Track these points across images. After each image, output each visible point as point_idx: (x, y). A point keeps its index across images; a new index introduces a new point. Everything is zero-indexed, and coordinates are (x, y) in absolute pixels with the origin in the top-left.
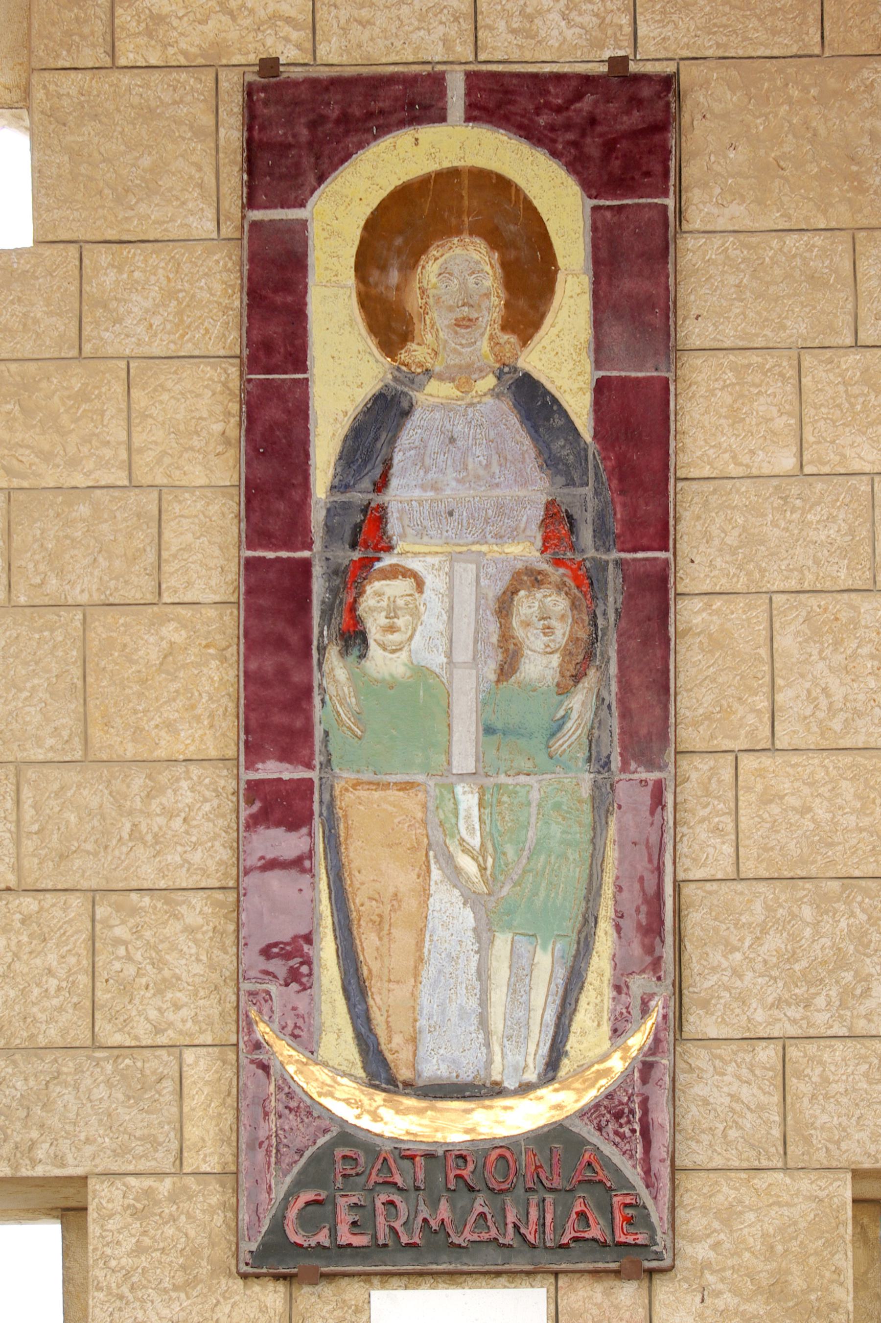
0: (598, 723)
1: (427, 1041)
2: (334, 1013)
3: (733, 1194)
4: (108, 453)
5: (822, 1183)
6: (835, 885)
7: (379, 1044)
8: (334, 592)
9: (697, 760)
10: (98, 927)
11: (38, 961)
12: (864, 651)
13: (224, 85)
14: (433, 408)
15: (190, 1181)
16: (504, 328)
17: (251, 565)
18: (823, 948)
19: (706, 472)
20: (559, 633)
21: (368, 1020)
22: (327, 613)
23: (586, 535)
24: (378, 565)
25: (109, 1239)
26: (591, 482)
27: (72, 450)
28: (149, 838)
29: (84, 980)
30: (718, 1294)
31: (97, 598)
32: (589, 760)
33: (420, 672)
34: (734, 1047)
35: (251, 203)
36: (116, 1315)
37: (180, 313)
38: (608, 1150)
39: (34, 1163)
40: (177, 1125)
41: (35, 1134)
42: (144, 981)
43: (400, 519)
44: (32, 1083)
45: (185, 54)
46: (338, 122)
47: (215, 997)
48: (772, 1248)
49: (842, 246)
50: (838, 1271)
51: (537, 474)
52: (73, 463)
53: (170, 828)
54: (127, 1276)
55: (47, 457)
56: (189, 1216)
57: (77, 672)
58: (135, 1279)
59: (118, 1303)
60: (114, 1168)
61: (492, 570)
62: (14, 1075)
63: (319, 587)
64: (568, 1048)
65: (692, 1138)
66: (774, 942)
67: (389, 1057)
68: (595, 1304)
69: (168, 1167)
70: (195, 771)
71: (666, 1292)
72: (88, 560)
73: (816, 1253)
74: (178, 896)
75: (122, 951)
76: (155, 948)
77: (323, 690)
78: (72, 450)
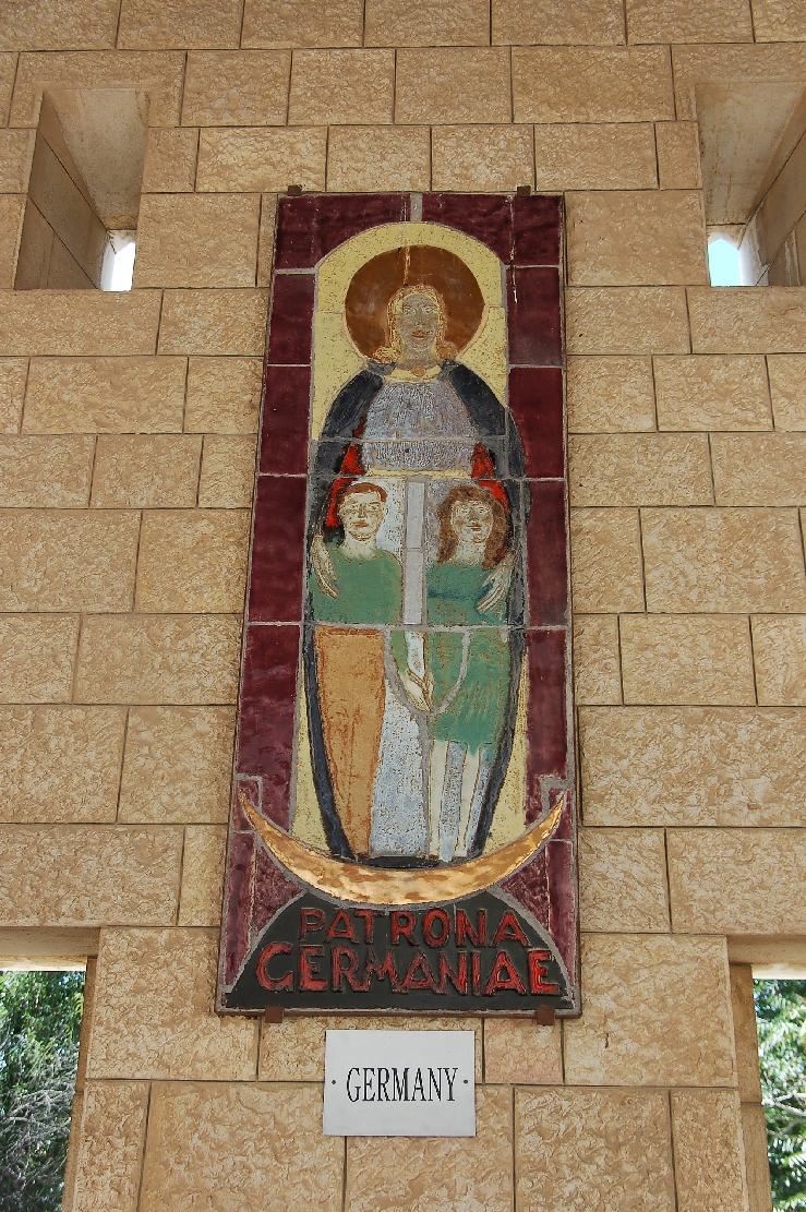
0: (513, 590)
1: (378, 821)
2: (306, 800)
3: (629, 953)
4: (169, 413)
5: (703, 946)
6: (699, 711)
7: (340, 825)
8: (321, 500)
9: (588, 619)
10: (130, 731)
11: (80, 757)
12: (711, 546)
13: (265, 203)
14: (396, 386)
15: (184, 933)
16: (447, 338)
17: (261, 481)
18: (692, 758)
19: (589, 429)
20: (484, 529)
21: (334, 805)
22: (316, 514)
23: (504, 465)
24: (354, 483)
25: (112, 981)
26: (507, 432)
27: (144, 411)
28: (175, 669)
29: (115, 771)
30: (620, 1040)
31: (152, 503)
32: (507, 616)
33: (381, 554)
34: (625, 833)
35: (278, 264)
36: (112, 1046)
37: (226, 329)
38: (524, 913)
39: (59, 915)
40: (177, 886)
41: (61, 892)
42: (161, 773)
43: (371, 454)
44: (64, 851)
45: (240, 185)
46: (338, 220)
47: (214, 788)
48: (663, 999)
49: (677, 295)
50: (721, 1023)
51: (468, 427)
52: (144, 418)
53: (191, 661)
54: (124, 1013)
55: (125, 414)
56: (179, 962)
57: (132, 552)
58: (131, 1015)
59: (115, 1037)
60: (123, 921)
61: (436, 487)
62: (51, 844)
63: (310, 496)
64: (491, 830)
65: (594, 906)
66: (654, 752)
67: (347, 833)
68: (516, 1047)
69: (165, 920)
70: (213, 622)
71: (576, 1038)
72: (150, 479)
73: (701, 1006)
74: (192, 710)
75: (145, 750)
76: (171, 748)
77: (310, 565)
78: (144, 411)
